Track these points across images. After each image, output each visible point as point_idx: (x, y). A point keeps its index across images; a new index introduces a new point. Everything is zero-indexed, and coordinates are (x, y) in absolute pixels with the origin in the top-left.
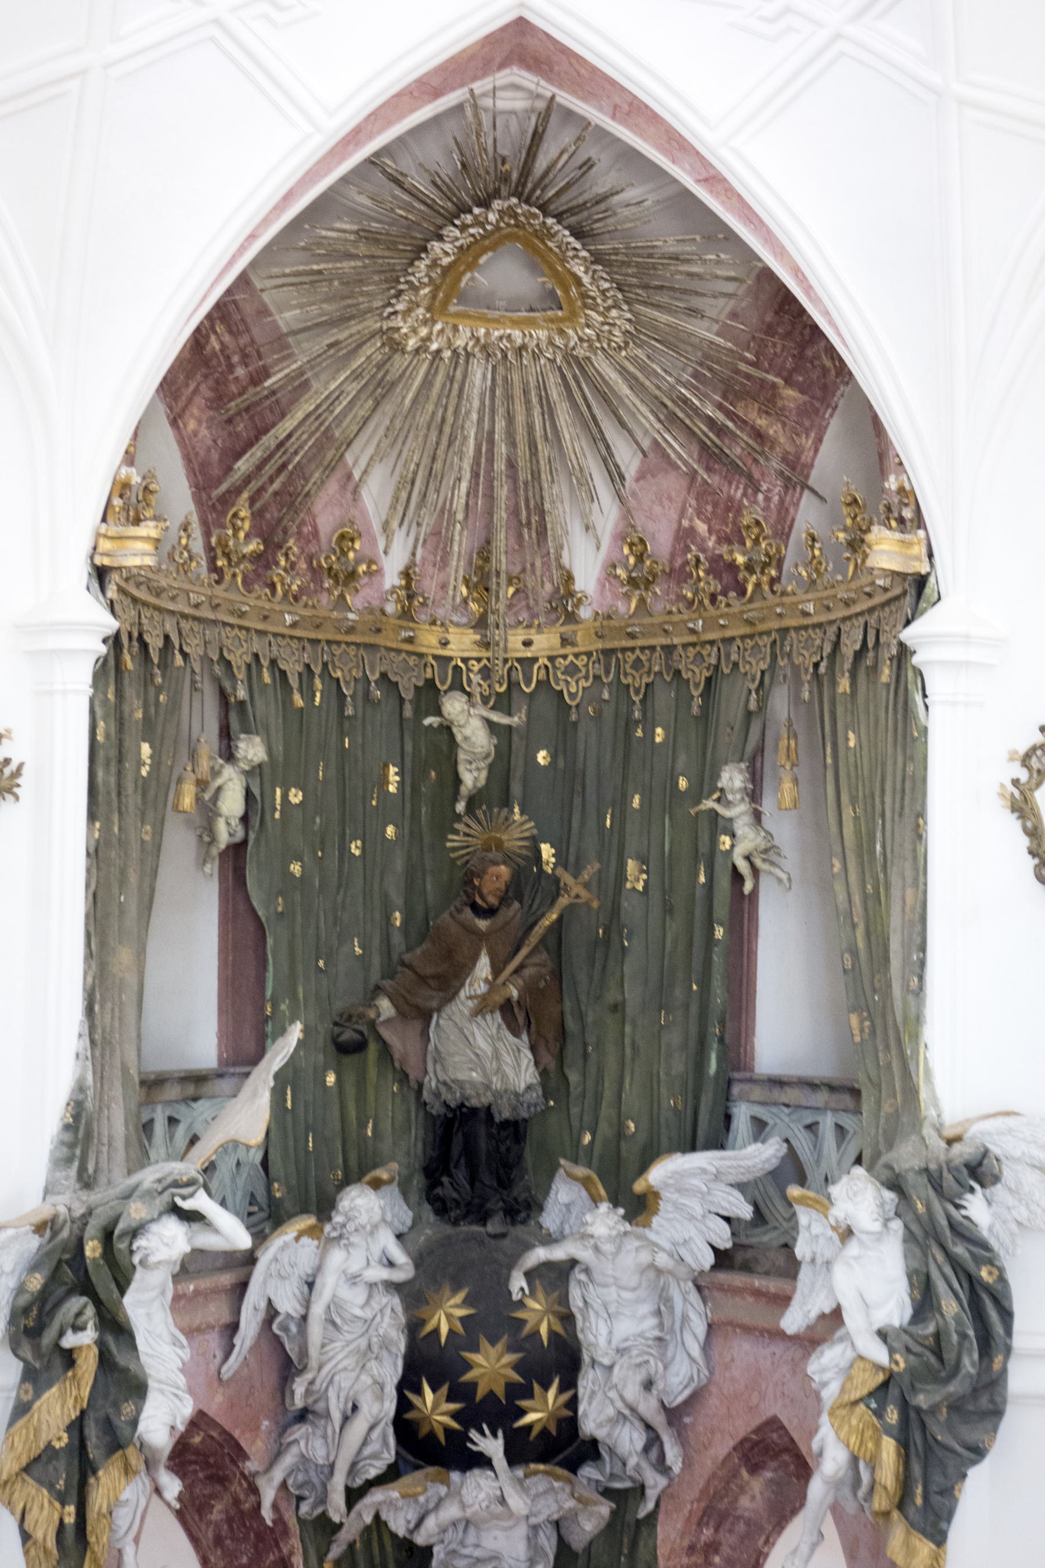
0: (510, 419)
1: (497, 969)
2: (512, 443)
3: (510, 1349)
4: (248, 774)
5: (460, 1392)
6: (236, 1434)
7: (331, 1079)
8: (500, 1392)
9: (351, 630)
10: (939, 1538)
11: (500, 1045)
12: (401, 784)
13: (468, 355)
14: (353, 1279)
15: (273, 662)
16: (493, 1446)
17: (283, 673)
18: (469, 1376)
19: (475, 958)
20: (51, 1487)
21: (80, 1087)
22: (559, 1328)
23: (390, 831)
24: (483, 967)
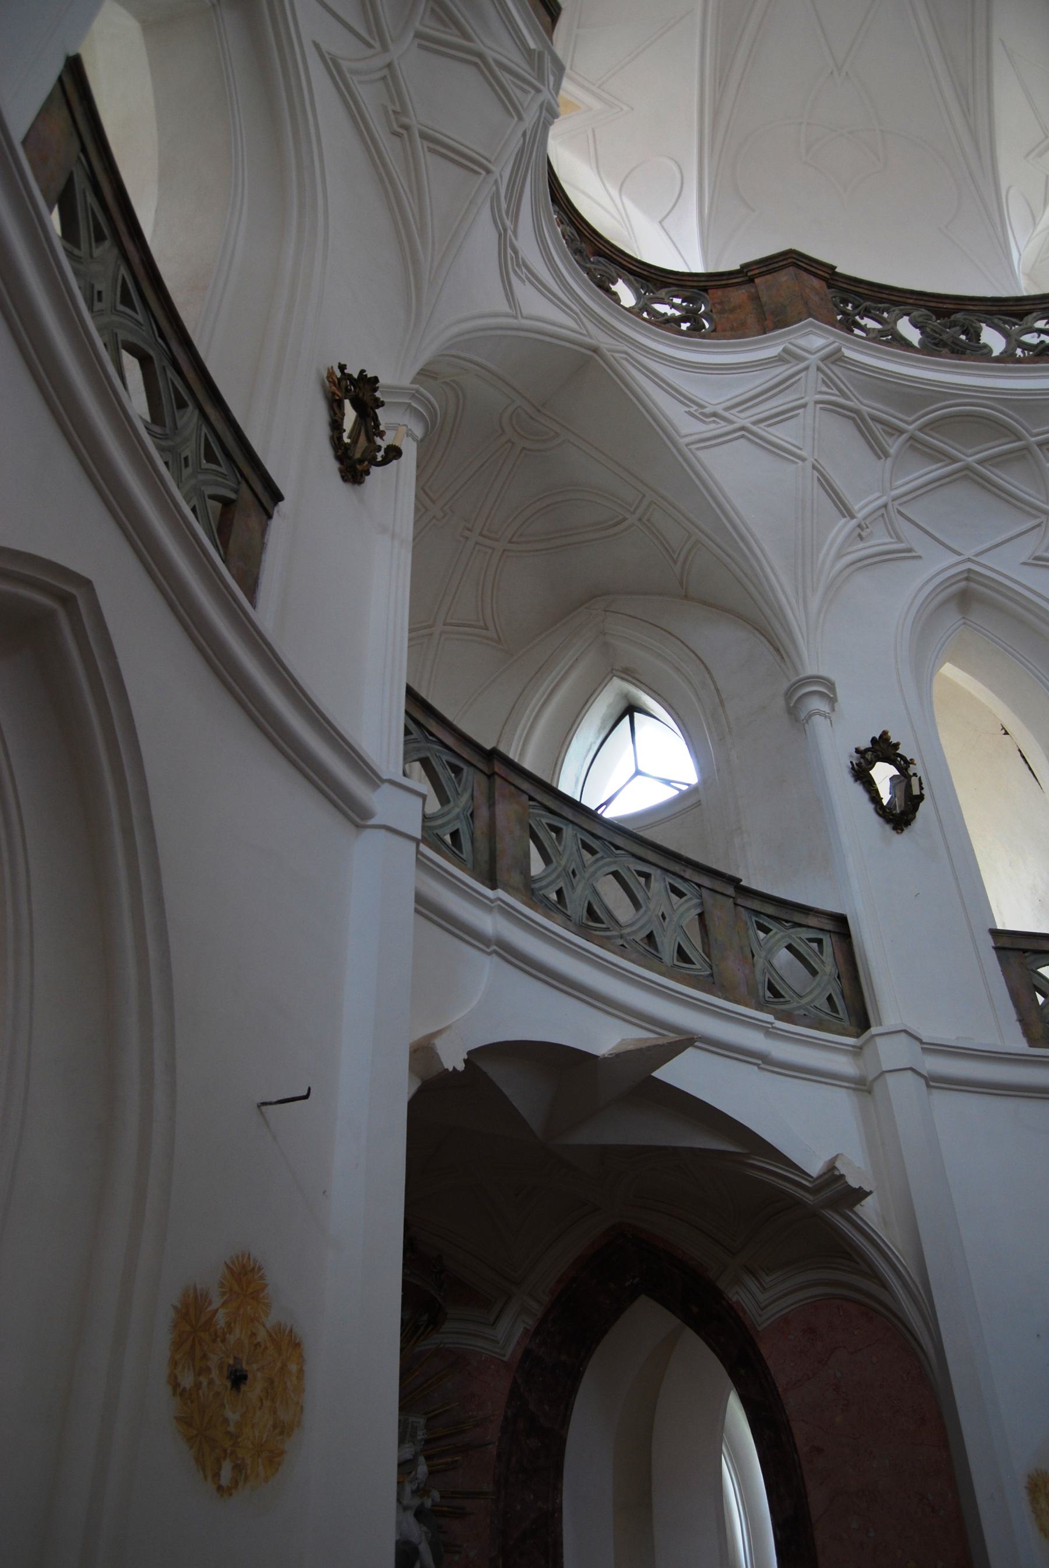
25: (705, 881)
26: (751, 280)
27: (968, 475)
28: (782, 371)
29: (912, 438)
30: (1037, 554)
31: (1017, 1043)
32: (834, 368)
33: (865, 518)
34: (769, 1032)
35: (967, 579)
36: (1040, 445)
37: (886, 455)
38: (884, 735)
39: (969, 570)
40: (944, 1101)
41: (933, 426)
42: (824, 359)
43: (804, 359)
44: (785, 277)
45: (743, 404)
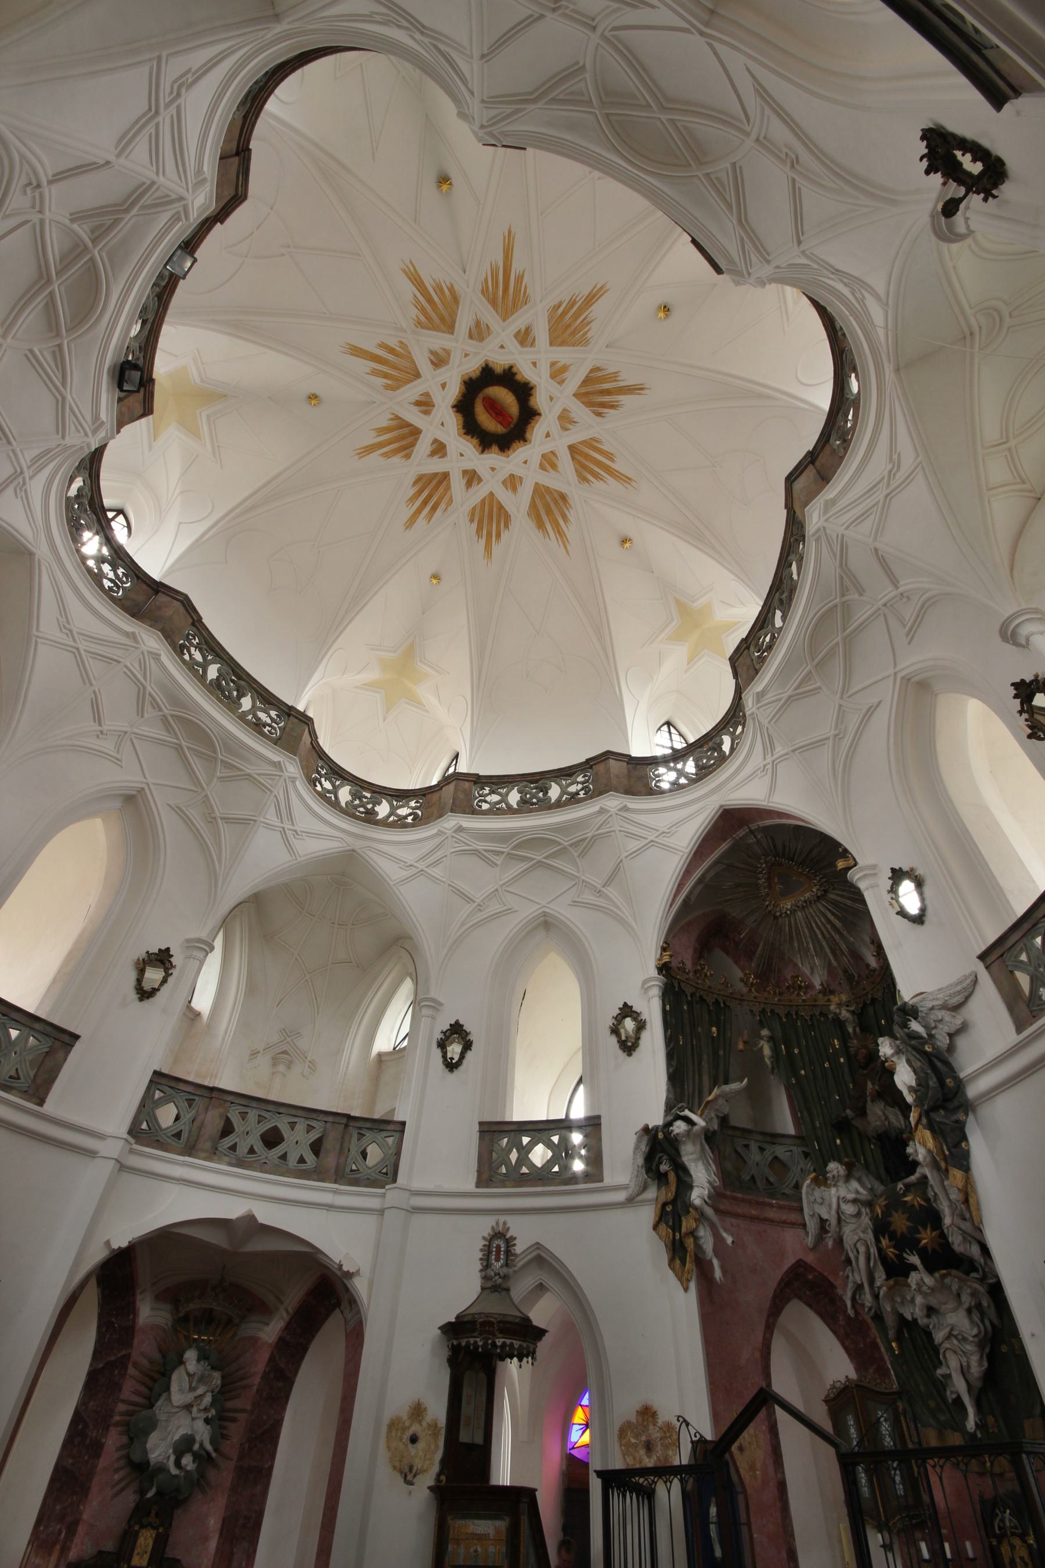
0: (816, 923)
1: (873, 1084)
2: (819, 929)
3: (903, 1213)
4: (768, 1041)
5: (892, 1236)
6: (826, 1274)
7: (838, 1141)
8: (905, 1230)
9: (804, 1001)
10: (966, 1169)
11: (886, 1112)
12: (839, 1045)
13: (794, 910)
14: (846, 1201)
15: (772, 1011)
16: (914, 1259)
17: (778, 1014)
18: (892, 1229)
19: (866, 1084)
20: (667, 1224)
21: (667, 1098)
22: (923, 1203)
23: (842, 1060)
24: (870, 1085)
25: (330, 1119)
26: (442, 788)
27: (540, 864)
28: (438, 840)
29: (509, 854)
30: (575, 899)
31: (469, 1184)
32: (461, 834)
33: (482, 901)
34: (336, 1192)
35: (545, 916)
36: (571, 845)
37: (497, 865)
38: (457, 1023)
39: (544, 912)
40: (418, 1220)
41: (517, 847)
42: (455, 832)
43: (446, 833)
44: (451, 787)
45: (422, 859)
